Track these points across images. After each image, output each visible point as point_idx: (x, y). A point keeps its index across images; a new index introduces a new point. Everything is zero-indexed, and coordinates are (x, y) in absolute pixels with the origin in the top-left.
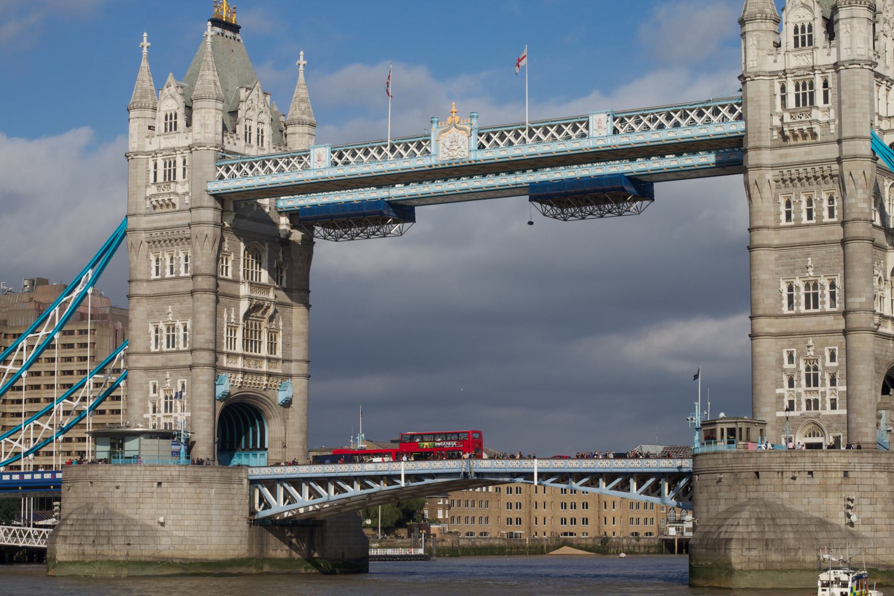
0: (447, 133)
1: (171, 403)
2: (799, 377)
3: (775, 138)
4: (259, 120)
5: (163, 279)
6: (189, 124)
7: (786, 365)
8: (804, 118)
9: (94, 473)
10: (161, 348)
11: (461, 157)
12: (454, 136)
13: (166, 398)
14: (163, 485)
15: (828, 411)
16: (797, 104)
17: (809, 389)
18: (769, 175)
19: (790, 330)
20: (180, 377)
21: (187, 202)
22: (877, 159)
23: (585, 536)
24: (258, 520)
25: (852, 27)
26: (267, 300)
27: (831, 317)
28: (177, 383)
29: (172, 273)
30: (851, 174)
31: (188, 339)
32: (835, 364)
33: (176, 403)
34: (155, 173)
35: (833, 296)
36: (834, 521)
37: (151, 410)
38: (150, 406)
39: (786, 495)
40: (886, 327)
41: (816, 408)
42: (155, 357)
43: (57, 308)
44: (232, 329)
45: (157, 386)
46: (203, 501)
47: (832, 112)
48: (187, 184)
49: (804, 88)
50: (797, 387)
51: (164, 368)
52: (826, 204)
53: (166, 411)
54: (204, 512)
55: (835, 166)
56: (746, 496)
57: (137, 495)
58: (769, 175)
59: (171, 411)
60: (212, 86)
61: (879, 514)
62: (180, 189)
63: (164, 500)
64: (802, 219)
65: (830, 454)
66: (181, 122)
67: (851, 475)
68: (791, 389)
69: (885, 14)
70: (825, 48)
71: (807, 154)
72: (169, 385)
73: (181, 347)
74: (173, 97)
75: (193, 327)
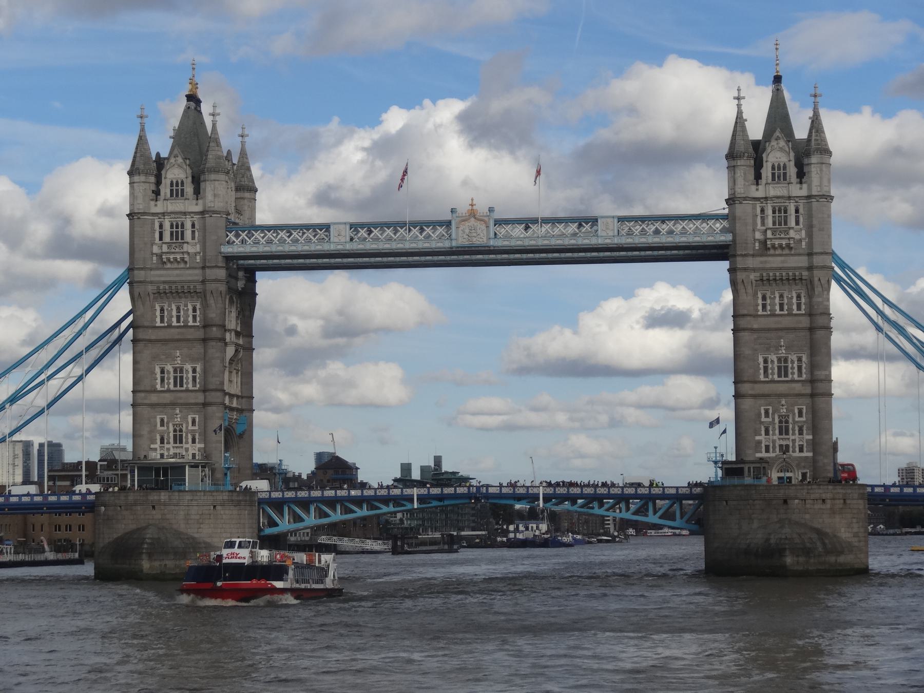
1: (181, 436)
3: (757, 248)
6: (197, 192)
7: (763, 419)
8: (782, 236)
9: (156, 498)
10: (168, 386)
11: (479, 243)
13: (175, 431)
14: (218, 508)
15: (797, 454)
17: (781, 437)
18: (753, 276)
20: (191, 413)
21: (198, 261)
24: (264, 536)
25: (821, 170)
27: (799, 385)
28: (187, 418)
30: (819, 280)
31: (198, 381)
32: (804, 419)
33: (187, 435)
35: (800, 368)
36: (839, 535)
37: (158, 441)
38: (158, 438)
45: (165, 421)
47: (803, 232)
48: (198, 246)
51: (173, 404)
52: (794, 300)
53: (175, 442)
55: (805, 274)
57: (197, 517)
62: (191, 250)
66: (189, 189)
67: (848, 502)
68: (767, 437)
70: (797, 183)
71: (783, 262)
72: (179, 420)
73: (190, 387)
74: (180, 166)
75: (205, 371)
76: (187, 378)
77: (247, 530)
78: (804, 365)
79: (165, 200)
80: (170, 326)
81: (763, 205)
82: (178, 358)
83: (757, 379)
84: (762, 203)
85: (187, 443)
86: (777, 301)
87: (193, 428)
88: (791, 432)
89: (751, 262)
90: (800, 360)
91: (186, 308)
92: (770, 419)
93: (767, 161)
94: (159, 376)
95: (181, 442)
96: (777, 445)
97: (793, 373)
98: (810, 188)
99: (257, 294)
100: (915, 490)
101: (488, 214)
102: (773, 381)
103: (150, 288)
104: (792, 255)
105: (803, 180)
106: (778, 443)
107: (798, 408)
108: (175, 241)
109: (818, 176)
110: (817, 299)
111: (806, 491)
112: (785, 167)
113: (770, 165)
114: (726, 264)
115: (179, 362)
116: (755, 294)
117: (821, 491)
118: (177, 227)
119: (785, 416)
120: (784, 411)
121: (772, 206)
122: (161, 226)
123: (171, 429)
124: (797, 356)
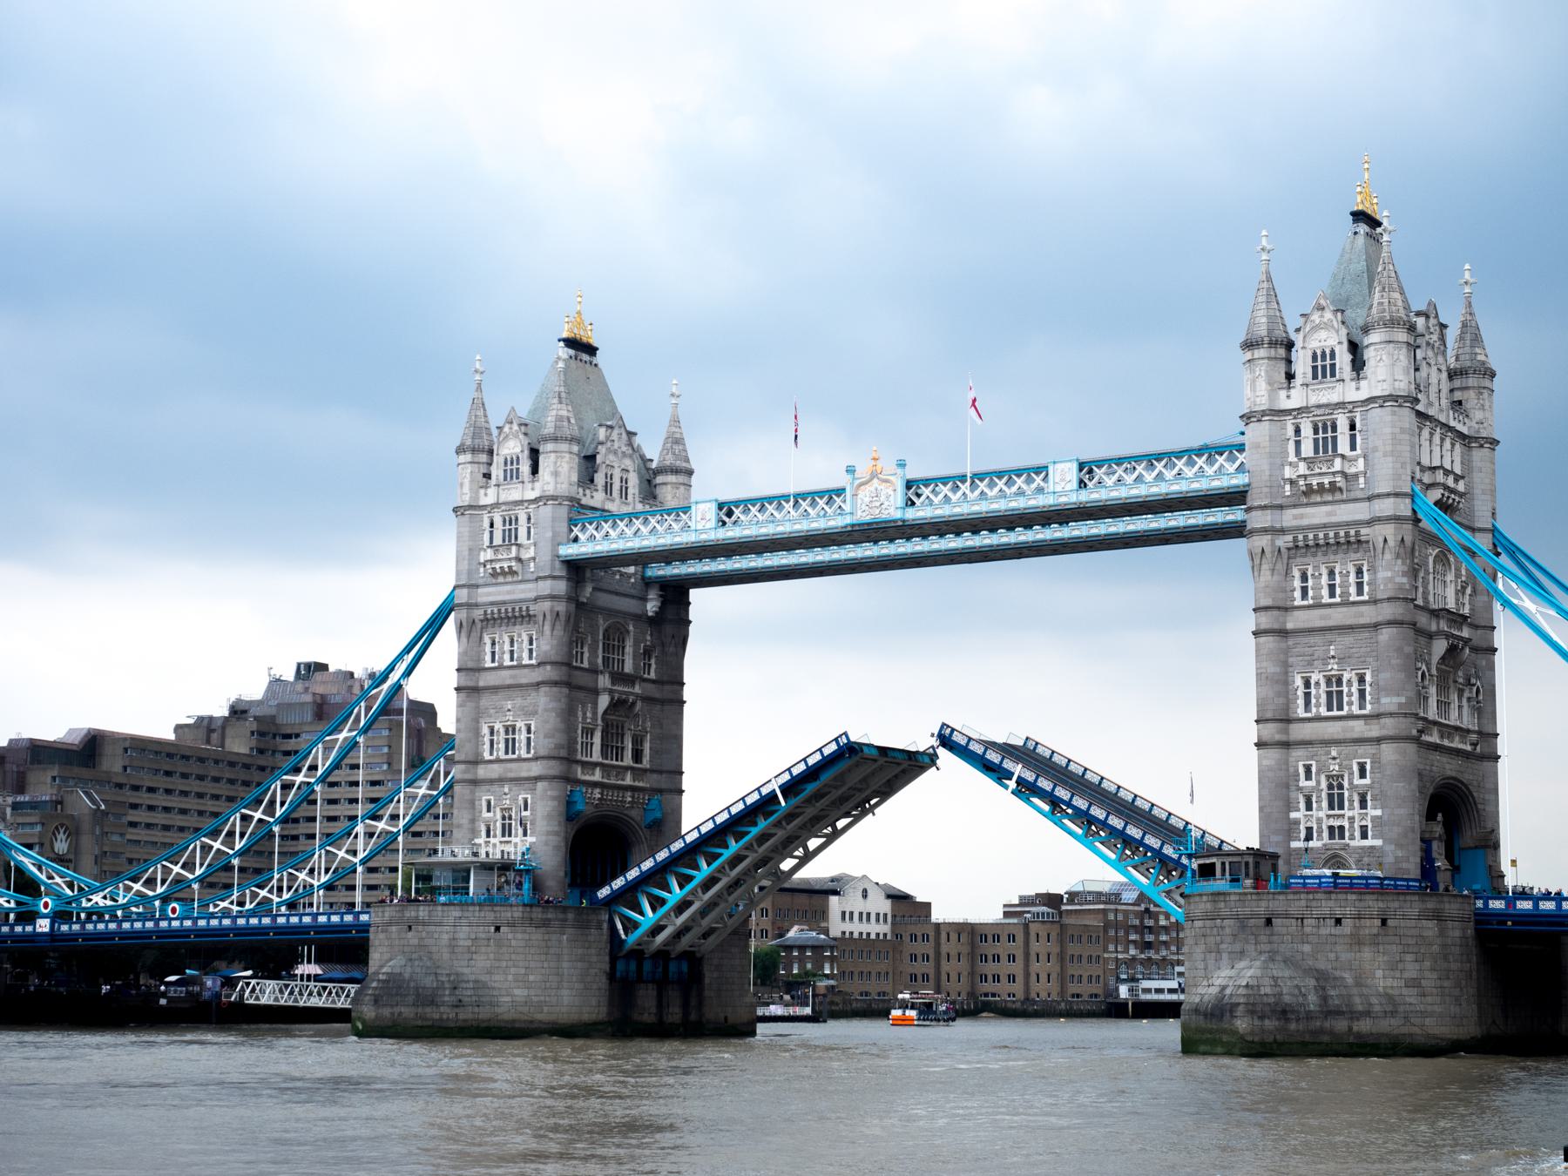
1: (510, 825)
2: (1319, 797)
3: (1288, 493)
4: (623, 467)
5: (501, 667)
6: (535, 470)
7: (1303, 783)
8: (1323, 470)
9: (413, 914)
13: (504, 818)
15: (1358, 842)
16: (1316, 451)
18: (1284, 541)
19: (1308, 738)
21: (532, 570)
26: (632, 694)
27: (1361, 722)
29: (512, 659)
30: (1385, 540)
31: (532, 744)
32: (1367, 781)
34: (491, 532)
35: (1362, 693)
37: (484, 833)
39: (1307, 948)
40: (1431, 735)
41: (1342, 837)
43: (363, 704)
44: (589, 732)
46: (552, 951)
47: (1361, 461)
48: (532, 548)
49: (1325, 431)
50: (1317, 810)
51: (501, 781)
52: (1352, 578)
53: (503, 835)
54: (553, 964)
56: (1256, 950)
57: (469, 943)
59: (510, 835)
60: (565, 424)
61: (1428, 974)
62: (525, 555)
63: (504, 949)
64: (1322, 597)
65: (1363, 897)
66: (525, 468)
67: (1390, 923)
69: (1427, 337)
70: (1352, 380)
71: (1329, 514)
72: (508, 802)
73: (525, 755)
75: (536, 727)
77: (565, 965)
78: (1368, 689)
81: (1298, 421)
83: (1295, 715)
84: (1295, 418)
85: (516, 836)
86: (1324, 580)
88: (1346, 803)
90: (1362, 680)
92: (1312, 783)
93: (1303, 348)
94: (487, 739)
96: (1324, 827)
97: (1350, 703)
98: (1370, 385)
99: (690, 622)
100: (1536, 905)
102: (1319, 719)
103: (478, 614)
104: (1344, 501)
107: (1359, 763)
109: (1381, 364)
111: (1303, 903)
113: (1310, 354)
115: (511, 718)
116: (1288, 572)
117: (1331, 903)
118: (510, 524)
119: (1338, 776)
121: (1312, 422)
123: (499, 816)
124: (1357, 674)
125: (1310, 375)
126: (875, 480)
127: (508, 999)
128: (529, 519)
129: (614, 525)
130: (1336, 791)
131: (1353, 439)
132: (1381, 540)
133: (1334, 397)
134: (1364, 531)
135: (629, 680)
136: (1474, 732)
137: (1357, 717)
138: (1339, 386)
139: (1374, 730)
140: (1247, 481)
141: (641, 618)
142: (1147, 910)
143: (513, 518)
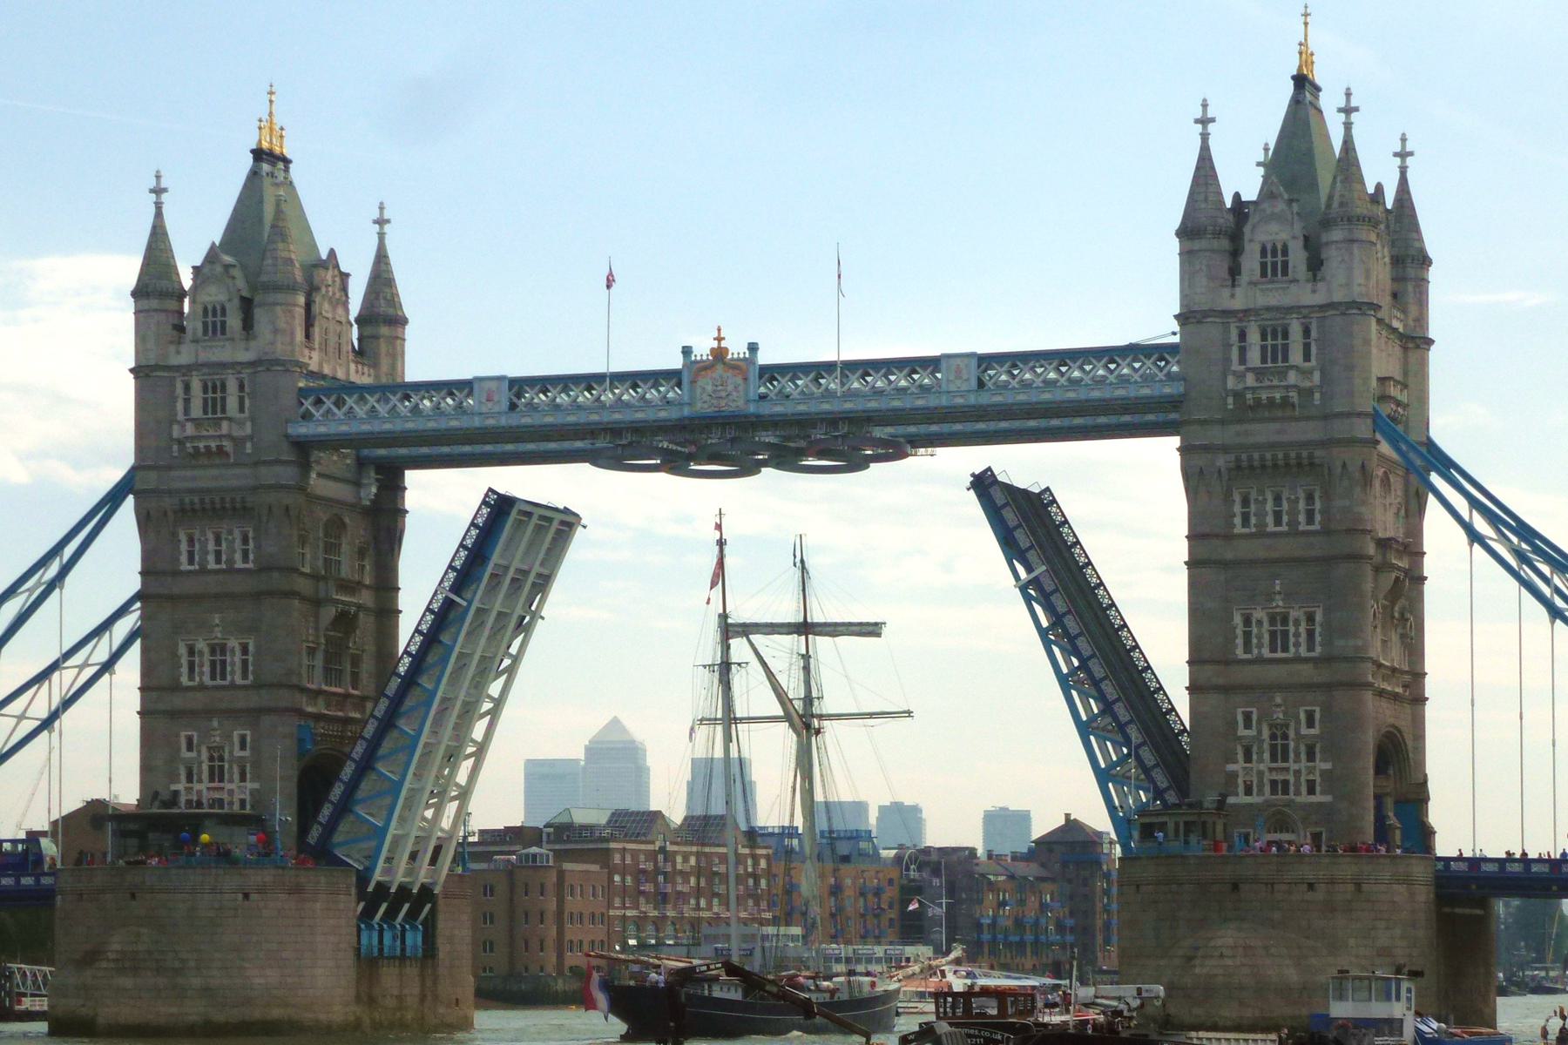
0: (709, 372)
1: (221, 768)
3: (1231, 407)
6: (248, 324)
7: (1242, 732)
8: (1275, 382)
10: (201, 679)
11: (731, 409)
12: (721, 377)
13: (211, 759)
14: (253, 897)
15: (1304, 798)
16: (1264, 360)
17: (1274, 765)
18: (1221, 461)
22: (1378, 442)
23: (488, 974)
27: (1311, 665)
30: (1344, 465)
31: (251, 668)
33: (231, 767)
34: (187, 401)
35: (1311, 634)
37: (183, 777)
41: (1286, 791)
42: (190, 695)
44: (312, 652)
45: (195, 741)
47: (1317, 377)
48: (249, 424)
49: (1275, 337)
51: (208, 713)
52: (1302, 505)
53: (212, 780)
58: (1221, 461)
62: (237, 433)
64: (1266, 525)
66: (234, 322)
67: (1365, 887)
70: (1308, 281)
72: (218, 739)
73: (239, 681)
76: (233, 664)
78: (1318, 630)
79: (193, 341)
80: (203, 571)
81: (1244, 324)
82: (217, 629)
85: (231, 781)
86: (1269, 506)
87: (242, 754)
88: (1292, 755)
89: (1216, 435)
90: (1310, 618)
91: (230, 537)
92: (1252, 732)
94: (184, 661)
95: (221, 780)
96: (1265, 780)
97: (1297, 645)
99: (407, 512)
101: (747, 356)
102: (1260, 661)
103: (168, 503)
104: (1297, 419)
105: (1319, 276)
106: (1267, 777)
107: (1306, 711)
108: (210, 416)
110: (1339, 503)
112: (1285, 252)
113: (1257, 248)
114: (1176, 441)
115: (219, 635)
119: (1282, 725)
120: (1279, 715)
121: (1259, 326)
122: (187, 388)
125: (1258, 272)
126: (720, 367)
127: (262, 981)
128: (241, 387)
129: (362, 399)
130: (1279, 742)
131: (1307, 347)
132: (1338, 464)
133: (1287, 300)
134: (1318, 453)
135: (349, 587)
136: (1407, 673)
137: (1307, 660)
138: (1293, 288)
139: (1322, 675)
140: (1182, 389)
141: (353, 507)
142: (663, 850)
143: (218, 384)
